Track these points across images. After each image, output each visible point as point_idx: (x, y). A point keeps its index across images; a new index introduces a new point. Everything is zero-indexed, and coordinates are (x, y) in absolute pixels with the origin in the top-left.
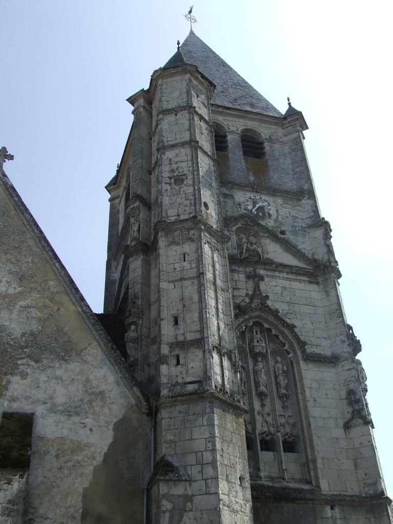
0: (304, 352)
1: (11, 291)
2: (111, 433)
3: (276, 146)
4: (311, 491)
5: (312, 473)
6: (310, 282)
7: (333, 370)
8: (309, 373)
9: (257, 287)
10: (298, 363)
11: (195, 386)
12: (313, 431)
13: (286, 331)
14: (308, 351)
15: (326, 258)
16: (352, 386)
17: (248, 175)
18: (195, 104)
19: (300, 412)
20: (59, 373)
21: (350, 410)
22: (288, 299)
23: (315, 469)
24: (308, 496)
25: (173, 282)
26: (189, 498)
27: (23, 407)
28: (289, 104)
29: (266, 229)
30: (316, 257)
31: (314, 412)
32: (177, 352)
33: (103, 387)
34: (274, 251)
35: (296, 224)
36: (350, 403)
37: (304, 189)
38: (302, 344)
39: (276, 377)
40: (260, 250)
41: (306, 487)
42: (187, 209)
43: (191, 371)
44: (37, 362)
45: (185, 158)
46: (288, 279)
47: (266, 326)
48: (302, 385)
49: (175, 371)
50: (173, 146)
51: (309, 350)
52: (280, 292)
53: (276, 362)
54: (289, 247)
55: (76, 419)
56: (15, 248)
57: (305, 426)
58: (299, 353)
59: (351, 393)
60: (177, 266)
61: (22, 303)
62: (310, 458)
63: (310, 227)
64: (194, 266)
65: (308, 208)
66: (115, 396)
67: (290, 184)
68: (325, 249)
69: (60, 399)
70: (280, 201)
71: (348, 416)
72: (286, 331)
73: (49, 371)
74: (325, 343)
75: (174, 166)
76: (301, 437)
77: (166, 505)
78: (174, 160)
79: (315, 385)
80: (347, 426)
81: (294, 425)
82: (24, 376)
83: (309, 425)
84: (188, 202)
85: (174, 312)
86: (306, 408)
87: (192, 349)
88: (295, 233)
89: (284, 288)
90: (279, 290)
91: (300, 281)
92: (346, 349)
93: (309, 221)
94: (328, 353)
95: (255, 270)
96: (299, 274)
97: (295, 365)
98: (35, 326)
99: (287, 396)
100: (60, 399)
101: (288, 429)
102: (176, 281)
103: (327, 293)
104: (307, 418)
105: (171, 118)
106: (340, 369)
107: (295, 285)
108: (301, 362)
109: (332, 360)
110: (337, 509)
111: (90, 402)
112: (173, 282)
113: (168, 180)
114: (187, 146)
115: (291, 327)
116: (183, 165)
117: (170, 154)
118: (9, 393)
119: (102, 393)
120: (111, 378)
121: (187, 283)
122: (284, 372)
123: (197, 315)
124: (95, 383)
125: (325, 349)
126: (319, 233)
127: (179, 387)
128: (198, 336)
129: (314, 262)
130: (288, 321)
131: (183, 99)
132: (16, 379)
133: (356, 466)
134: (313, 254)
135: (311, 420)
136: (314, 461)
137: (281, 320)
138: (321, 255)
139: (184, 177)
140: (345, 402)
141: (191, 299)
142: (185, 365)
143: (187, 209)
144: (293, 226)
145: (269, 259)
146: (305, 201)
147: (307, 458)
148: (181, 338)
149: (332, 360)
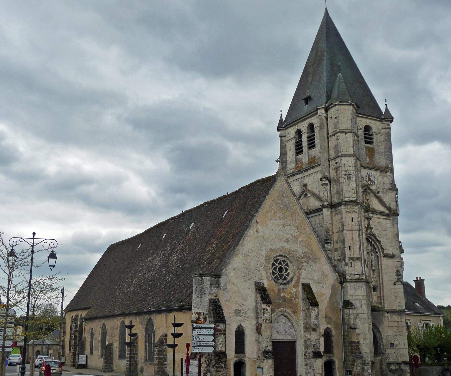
0: (383, 253)
1: (296, 234)
2: (330, 290)
3: (378, 136)
4: (382, 308)
5: (382, 301)
6: (387, 219)
7: (392, 260)
8: (385, 261)
9: (369, 224)
10: (381, 257)
11: (358, 276)
12: (384, 286)
13: (378, 244)
14: (385, 252)
15: (395, 208)
16: (399, 268)
17: (366, 158)
18: (336, 95)
19: (379, 277)
20: (314, 268)
21: (397, 278)
22: (379, 228)
23: (384, 299)
24: (381, 309)
25: (348, 230)
26: (357, 314)
27: (306, 281)
28: (386, 107)
29: (373, 193)
30: (391, 206)
31: (385, 278)
32: (351, 261)
33: (327, 273)
34: (376, 205)
35: (384, 187)
36: (397, 275)
37: (389, 166)
38: (383, 249)
39: (372, 262)
40: (370, 203)
41: (380, 306)
42: (353, 195)
43: (356, 270)
44: (308, 264)
45: (351, 165)
46: (380, 218)
47: (371, 241)
48: (381, 267)
49: (351, 269)
50: (346, 156)
51: (385, 252)
52: (376, 225)
53: (372, 255)
54: (381, 201)
55: (321, 285)
56: (294, 213)
57: (381, 283)
58: (381, 253)
59: (398, 271)
60: (350, 223)
61: (299, 239)
62: (382, 295)
63: (390, 189)
64: (357, 225)
65: (390, 178)
66: (332, 277)
67: (382, 162)
68: (395, 203)
69: (316, 278)
70: (378, 173)
71: (396, 280)
72: (378, 244)
73: (311, 267)
74: (390, 249)
75: (347, 169)
76: (379, 287)
77: (352, 316)
78: (347, 164)
79: (386, 267)
80: (395, 284)
81: (376, 281)
82: (305, 270)
83: (383, 283)
84: (353, 191)
85: (349, 245)
86: (382, 276)
87: (357, 261)
88: (383, 192)
89: (378, 223)
90: (376, 224)
91: (383, 219)
92: (397, 252)
93: (389, 186)
94: (391, 253)
95: (368, 215)
96: (383, 215)
97: (379, 258)
98: (305, 249)
99: (374, 270)
100: (316, 278)
101: (374, 283)
102: (350, 230)
103: (393, 225)
104: (382, 280)
105: (343, 136)
106: (395, 260)
107: (382, 221)
108: (382, 257)
109: (392, 256)
110: (389, 314)
111: (324, 278)
112: (348, 230)
113: (343, 176)
114: (352, 157)
115: (379, 242)
116: (350, 168)
117: (344, 160)
118: (302, 276)
119: (327, 275)
120: (329, 270)
121: (354, 232)
122: (375, 260)
123: (358, 247)
124: (324, 271)
125: (389, 251)
126: (393, 194)
127: (352, 275)
128: (359, 256)
129: (389, 209)
130: (379, 239)
131: (349, 124)
132: (303, 271)
133: (396, 299)
134: (389, 204)
135: (384, 281)
136: (383, 297)
137: (376, 239)
138: (393, 206)
139: (351, 176)
140: (395, 274)
141: (356, 240)
142: (354, 267)
143: (353, 195)
144: (383, 189)
145: (373, 208)
146: (388, 174)
147: (380, 294)
148: (352, 256)
149: (392, 256)
